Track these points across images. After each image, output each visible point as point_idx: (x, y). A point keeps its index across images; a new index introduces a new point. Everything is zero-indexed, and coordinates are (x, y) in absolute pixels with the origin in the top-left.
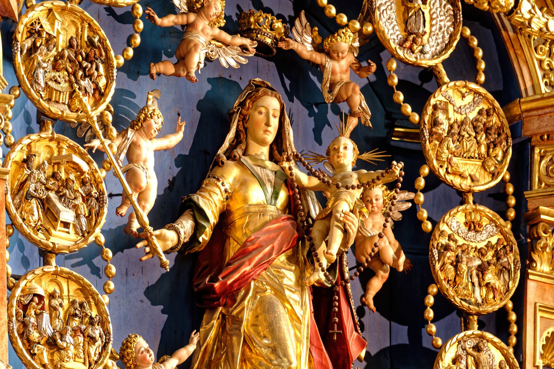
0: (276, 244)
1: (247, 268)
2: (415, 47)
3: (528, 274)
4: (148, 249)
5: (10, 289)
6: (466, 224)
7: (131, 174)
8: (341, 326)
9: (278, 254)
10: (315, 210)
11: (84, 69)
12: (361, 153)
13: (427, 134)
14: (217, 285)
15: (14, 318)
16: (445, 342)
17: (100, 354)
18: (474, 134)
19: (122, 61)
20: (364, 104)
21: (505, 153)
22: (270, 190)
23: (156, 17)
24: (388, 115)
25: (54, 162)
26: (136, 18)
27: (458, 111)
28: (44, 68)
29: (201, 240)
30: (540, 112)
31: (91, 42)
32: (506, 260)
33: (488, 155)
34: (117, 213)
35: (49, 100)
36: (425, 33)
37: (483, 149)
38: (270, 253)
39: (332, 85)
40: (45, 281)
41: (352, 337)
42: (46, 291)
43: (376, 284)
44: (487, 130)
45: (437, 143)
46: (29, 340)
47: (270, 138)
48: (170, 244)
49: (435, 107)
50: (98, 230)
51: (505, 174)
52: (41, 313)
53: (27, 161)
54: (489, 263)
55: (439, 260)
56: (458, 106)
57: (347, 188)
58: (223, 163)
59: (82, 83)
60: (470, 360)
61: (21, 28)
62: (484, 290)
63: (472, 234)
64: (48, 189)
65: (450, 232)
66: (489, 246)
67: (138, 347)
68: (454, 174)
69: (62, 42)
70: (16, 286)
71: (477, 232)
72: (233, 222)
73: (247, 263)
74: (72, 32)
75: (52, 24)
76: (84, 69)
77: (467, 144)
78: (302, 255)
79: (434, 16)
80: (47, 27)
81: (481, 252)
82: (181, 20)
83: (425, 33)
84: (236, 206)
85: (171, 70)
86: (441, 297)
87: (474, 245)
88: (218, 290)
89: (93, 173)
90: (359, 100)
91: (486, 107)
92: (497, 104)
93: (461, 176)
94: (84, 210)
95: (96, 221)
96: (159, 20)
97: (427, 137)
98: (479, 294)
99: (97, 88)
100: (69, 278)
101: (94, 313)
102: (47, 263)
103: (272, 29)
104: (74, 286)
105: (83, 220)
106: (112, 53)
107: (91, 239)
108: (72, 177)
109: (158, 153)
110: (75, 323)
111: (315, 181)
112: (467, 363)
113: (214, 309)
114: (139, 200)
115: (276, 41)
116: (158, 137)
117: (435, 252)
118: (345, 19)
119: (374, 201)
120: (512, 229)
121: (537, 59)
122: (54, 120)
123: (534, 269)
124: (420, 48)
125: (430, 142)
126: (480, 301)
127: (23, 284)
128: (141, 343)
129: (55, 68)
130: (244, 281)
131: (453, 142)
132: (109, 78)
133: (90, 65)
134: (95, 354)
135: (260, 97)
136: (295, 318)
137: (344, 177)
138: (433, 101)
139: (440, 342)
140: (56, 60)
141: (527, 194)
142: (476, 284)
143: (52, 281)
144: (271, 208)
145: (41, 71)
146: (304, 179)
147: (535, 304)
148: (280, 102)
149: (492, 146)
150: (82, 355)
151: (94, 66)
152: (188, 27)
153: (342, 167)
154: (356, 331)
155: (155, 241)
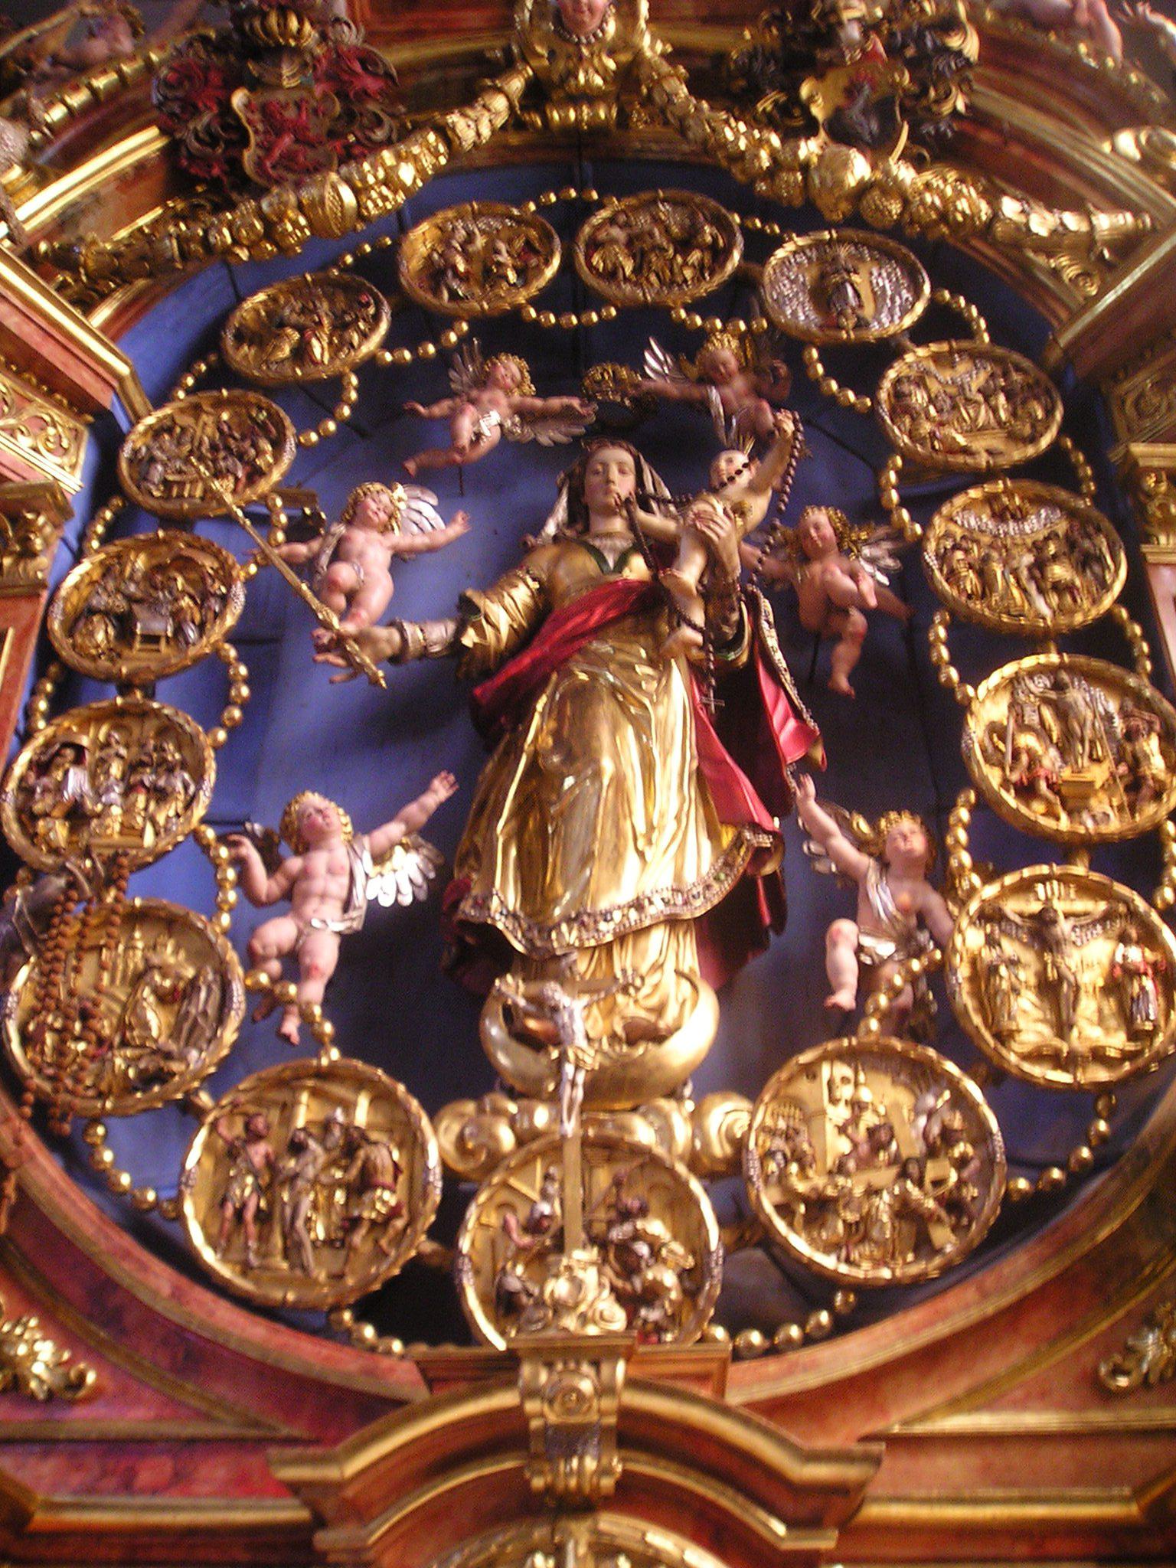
3: (1143, 556)
21: (1049, 412)
37: (1003, 415)
60: (1048, 714)
62: (1054, 599)
81: (1038, 548)
93: (966, 451)
98: (1043, 607)
138: (892, 374)
143: (116, 727)
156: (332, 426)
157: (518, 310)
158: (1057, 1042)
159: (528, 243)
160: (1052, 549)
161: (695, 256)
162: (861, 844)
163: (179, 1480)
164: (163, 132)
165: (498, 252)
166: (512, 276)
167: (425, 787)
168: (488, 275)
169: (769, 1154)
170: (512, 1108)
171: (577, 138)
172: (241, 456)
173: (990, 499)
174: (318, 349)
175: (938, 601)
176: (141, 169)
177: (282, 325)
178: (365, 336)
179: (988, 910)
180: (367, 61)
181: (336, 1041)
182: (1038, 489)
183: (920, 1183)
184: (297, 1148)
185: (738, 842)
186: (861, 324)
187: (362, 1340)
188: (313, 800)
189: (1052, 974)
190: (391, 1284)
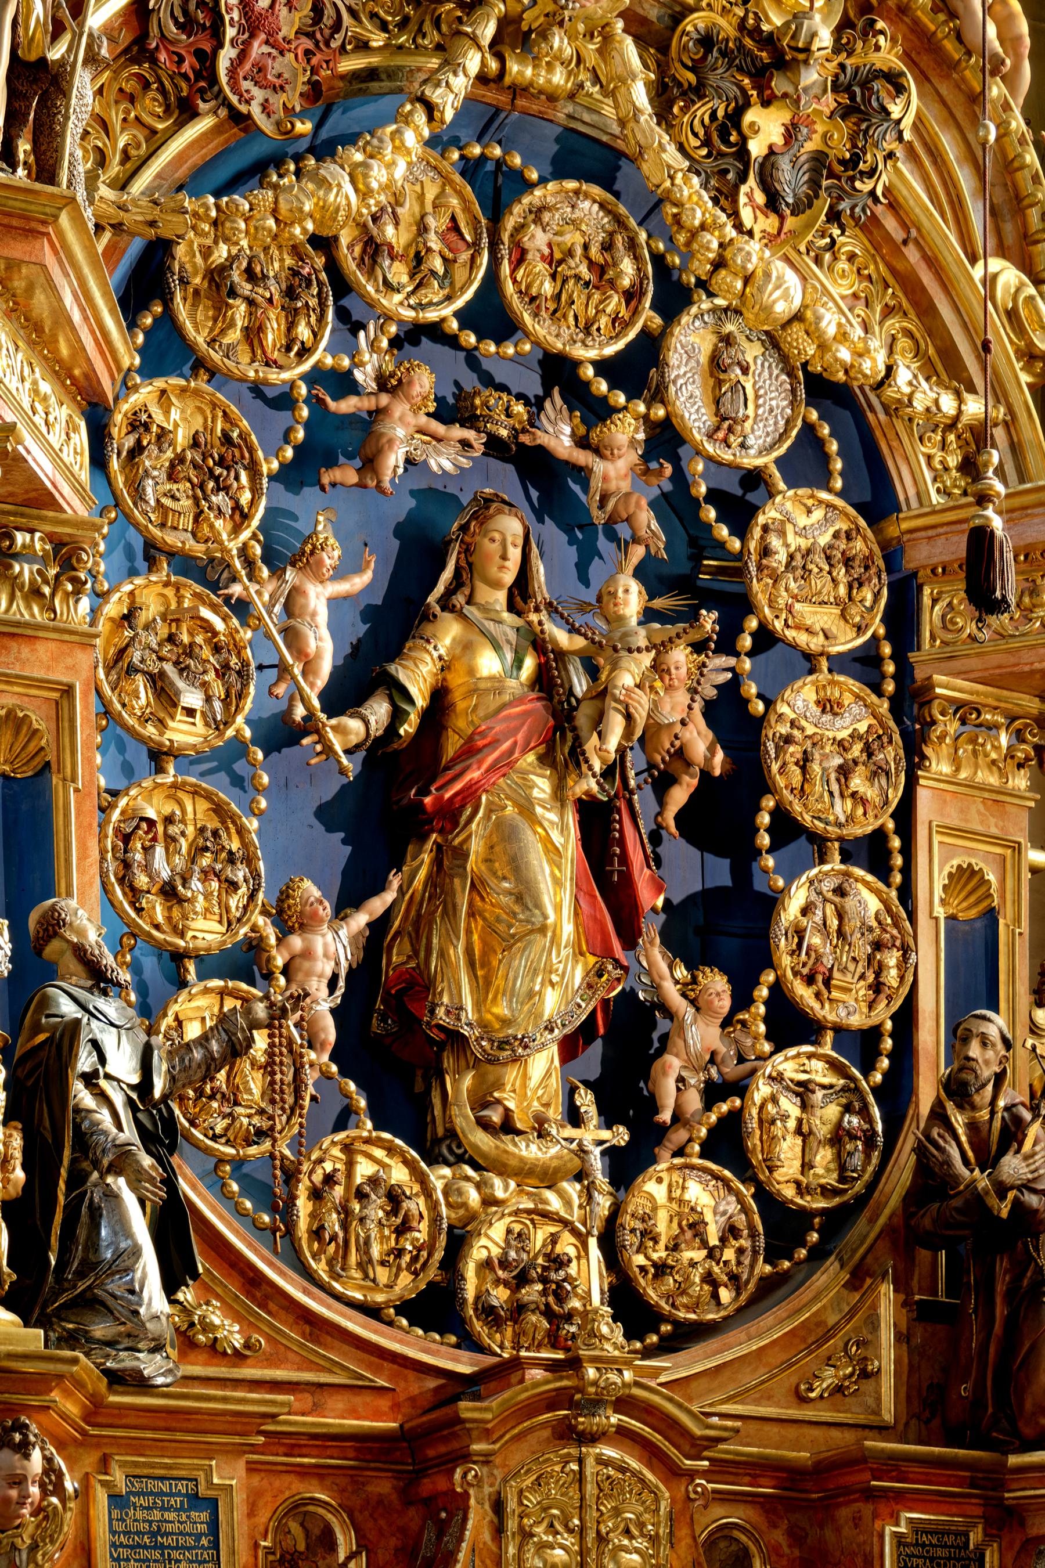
0: (520, 737)
1: (475, 774)
2: (732, 438)
3: (917, 778)
4: (319, 748)
5: (102, 810)
6: (818, 703)
7: (292, 636)
8: (624, 859)
9: (525, 751)
10: (580, 685)
11: (217, 479)
12: (651, 598)
13: (753, 568)
14: (428, 800)
15: (110, 855)
17: (245, 908)
18: (827, 568)
19: (275, 465)
20: (655, 525)
21: (877, 596)
22: (509, 656)
23: (328, 399)
24: (693, 542)
26: (297, 401)
27: (803, 532)
28: (153, 478)
29: (402, 732)
30: (930, 533)
31: (226, 439)
32: (882, 756)
33: (850, 599)
34: (271, 693)
35: (163, 525)
36: (748, 417)
37: (842, 590)
38: (511, 751)
39: (604, 499)
40: (158, 797)
41: (642, 876)
42: (159, 813)
43: (679, 796)
44: (848, 562)
45: (770, 582)
46: (133, 889)
48: (354, 740)
49: (766, 529)
50: (240, 719)
52: (152, 847)
53: (128, 618)
54: (855, 762)
55: (777, 758)
56: (802, 526)
57: (630, 651)
58: (435, 616)
59: (214, 499)
60: (830, 909)
61: (118, 418)
62: (849, 803)
63: (827, 718)
64: (161, 659)
65: (793, 716)
66: (855, 736)
67: (306, 896)
68: (798, 628)
69: (182, 438)
70: (112, 806)
71: (835, 714)
72: (453, 705)
73: (475, 767)
74: (198, 424)
75: (167, 413)
76: (217, 479)
78: (562, 754)
79: (762, 392)
80: (158, 417)
81: (842, 746)
83: (748, 417)
84: (457, 680)
85: (353, 478)
86: (780, 814)
87: (830, 734)
88: (429, 808)
89: (232, 633)
90: (646, 519)
91: (845, 527)
92: (862, 522)
93: (808, 630)
94: (218, 689)
95: (237, 706)
96: (332, 405)
97: (754, 573)
98: (841, 809)
99: (237, 507)
100: (196, 792)
101: (235, 845)
102: (160, 770)
103: (508, 416)
104: (203, 805)
105: (217, 705)
106: (260, 454)
107: (230, 733)
108: (199, 639)
110: (206, 860)
111: (580, 642)
112: (824, 913)
113: (424, 838)
114: (304, 673)
115: (515, 432)
116: (332, 579)
117: (771, 746)
118: (621, 399)
119: (673, 671)
120: (891, 710)
121: (924, 454)
122: (171, 554)
123: (927, 769)
124: (740, 440)
125: (759, 580)
126: (842, 819)
127: (123, 802)
128: (310, 889)
129: (172, 477)
130: (471, 794)
131: (795, 580)
132: (255, 490)
133: (225, 473)
134: (237, 908)
135: (492, 517)
136: (553, 852)
137: (625, 635)
138: (761, 519)
139: (781, 883)
140: (172, 466)
142: (837, 794)
143: (168, 797)
144: (512, 683)
145: (150, 482)
146: (562, 638)
147: (930, 822)
148: (523, 524)
149: (856, 585)
150: (216, 910)
151: (232, 474)
152: (378, 414)
153: (621, 619)
154: (649, 867)
155: (331, 735)
158: (801, 1178)
159: (453, 219)
165: (422, 228)
166: (438, 265)
169: (633, 1231)
174: (272, 337)
179: (774, 1074)
183: (718, 1264)
184: (361, 1195)
187: (401, 1328)
189: (805, 1129)
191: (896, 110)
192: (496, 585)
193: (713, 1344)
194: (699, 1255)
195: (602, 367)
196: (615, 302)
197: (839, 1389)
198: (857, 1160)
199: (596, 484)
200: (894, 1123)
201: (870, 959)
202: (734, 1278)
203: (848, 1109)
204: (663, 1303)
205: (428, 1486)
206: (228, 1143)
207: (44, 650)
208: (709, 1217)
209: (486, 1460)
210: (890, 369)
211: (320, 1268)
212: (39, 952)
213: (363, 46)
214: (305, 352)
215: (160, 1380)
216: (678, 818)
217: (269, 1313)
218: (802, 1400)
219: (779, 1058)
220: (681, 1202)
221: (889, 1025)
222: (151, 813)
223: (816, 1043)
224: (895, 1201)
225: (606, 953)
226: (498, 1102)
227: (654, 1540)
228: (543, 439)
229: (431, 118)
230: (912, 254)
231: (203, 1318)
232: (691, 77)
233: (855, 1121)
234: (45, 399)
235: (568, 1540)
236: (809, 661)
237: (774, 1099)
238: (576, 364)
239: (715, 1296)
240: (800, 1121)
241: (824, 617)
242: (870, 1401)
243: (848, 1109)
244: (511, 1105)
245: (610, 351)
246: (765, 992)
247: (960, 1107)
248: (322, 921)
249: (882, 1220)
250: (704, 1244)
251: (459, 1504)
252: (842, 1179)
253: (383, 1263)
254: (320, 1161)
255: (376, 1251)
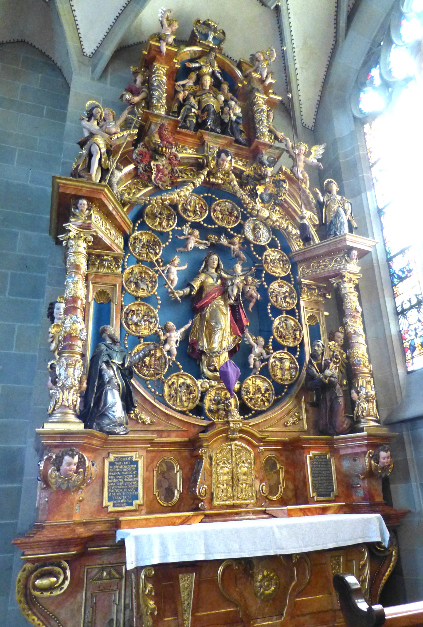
0: (217, 293)
11: (151, 247)
13: (264, 262)
16: (275, 319)
19: (164, 246)
21: (289, 267)
22: (215, 280)
25: (141, 273)
27: (273, 256)
35: (139, 256)
37: (282, 266)
44: (282, 261)
46: (128, 324)
47: (215, 266)
49: (266, 255)
50: (154, 291)
51: (289, 271)
53: (131, 273)
54: (287, 296)
66: (287, 292)
69: (145, 241)
77: (276, 264)
81: (284, 293)
82: (186, 237)
86: (273, 307)
93: (276, 273)
94: (150, 285)
98: (285, 305)
109: (177, 271)
118: (236, 234)
127: (127, 307)
132: (160, 250)
138: (265, 254)
141: (298, 277)
155: (176, 294)
156: (167, 244)
157: (200, 222)
159: (202, 205)
160: (287, 294)
161: (233, 218)
162: (253, 340)
163: (168, 436)
164: (134, 165)
165: (196, 207)
167: (187, 323)
168: (195, 212)
169: (244, 391)
170: (208, 381)
171: (213, 184)
172: (153, 249)
173: (278, 283)
174: (164, 224)
175: (269, 301)
176: (129, 173)
177: (156, 216)
178: (173, 224)
180: (176, 156)
181: (182, 369)
182: (286, 282)
184: (180, 387)
185: (236, 338)
186: (260, 242)
188: (171, 324)
190: (195, 408)
191: (284, 185)
192: (213, 268)
193: (264, 415)
194: (260, 395)
195: (231, 229)
196: (233, 218)
197: (294, 423)
198: (294, 373)
199: (233, 250)
200: (301, 365)
201: (293, 333)
202: (268, 400)
203: (291, 363)
204: (252, 407)
205: (195, 453)
206: (148, 376)
207: (110, 278)
208: (261, 387)
209: (207, 447)
210: (287, 227)
211: (170, 404)
212: (101, 336)
213: (183, 177)
214: (171, 226)
215: (122, 433)
216: (252, 309)
217: (157, 414)
218: (286, 426)
219: (275, 353)
220: (255, 384)
221: (298, 346)
222: (134, 309)
223: (283, 350)
224: (303, 381)
225: (237, 334)
226: (213, 365)
227: (250, 463)
228: (221, 242)
229: (194, 186)
230: (290, 210)
231: (140, 417)
232: (246, 181)
233: (293, 365)
234: (109, 230)
235: (228, 466)
236: (276, 278)
237: (275, 362)
238: (227, 229)
239: (264, 404)
240: (281, 366)
241: (278, 271)
242: (301, 425)
243: (291, 363)
244: (216, 365)
245: (233, 226)
246: (271, 340)
247: (315, 361)
248: (173, 330)
249: (300, 386)
250: (261, 393)
251: (201, 458)
252: (291, 377)
253: (186, 401)
254: (170, 379)
255: (184, 399)
